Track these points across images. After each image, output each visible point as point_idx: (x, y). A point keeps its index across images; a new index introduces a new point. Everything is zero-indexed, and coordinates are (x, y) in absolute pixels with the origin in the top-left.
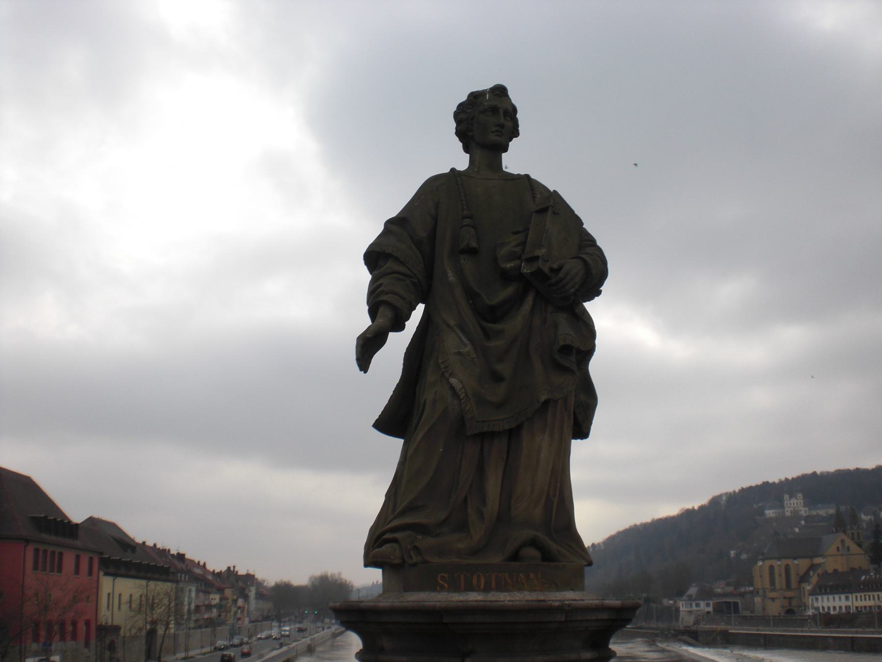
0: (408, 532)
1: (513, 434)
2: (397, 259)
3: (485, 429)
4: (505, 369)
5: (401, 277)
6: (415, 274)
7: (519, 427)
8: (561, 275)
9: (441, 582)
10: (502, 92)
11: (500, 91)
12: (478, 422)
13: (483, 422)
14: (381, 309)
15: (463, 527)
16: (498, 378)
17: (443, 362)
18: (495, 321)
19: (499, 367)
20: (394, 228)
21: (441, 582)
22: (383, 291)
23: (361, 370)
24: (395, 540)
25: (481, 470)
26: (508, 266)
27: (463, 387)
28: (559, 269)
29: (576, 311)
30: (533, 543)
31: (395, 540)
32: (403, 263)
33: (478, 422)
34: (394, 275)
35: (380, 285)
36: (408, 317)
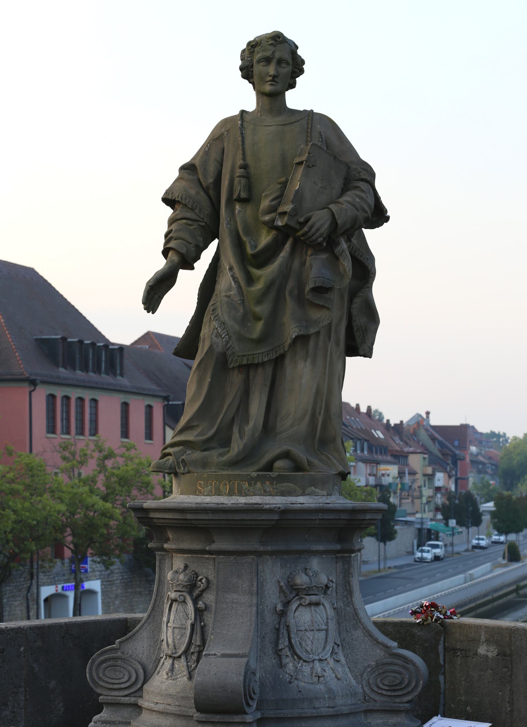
0: (181, 447)
3: (245, 362)
5: (190, 222)
6: (203, 219)
9: (199, 488)
10: (275, 40)
12: (239, 356)
13: (244, 356)
15: (226, 443)
21: (199, 488)
22: (172, 237)
26: (267, 218)
29: (335, 251)
30: (286, 455)
32: (192, 209)
33: (239, 356)
34: (184, 221)
36: (198, 258)
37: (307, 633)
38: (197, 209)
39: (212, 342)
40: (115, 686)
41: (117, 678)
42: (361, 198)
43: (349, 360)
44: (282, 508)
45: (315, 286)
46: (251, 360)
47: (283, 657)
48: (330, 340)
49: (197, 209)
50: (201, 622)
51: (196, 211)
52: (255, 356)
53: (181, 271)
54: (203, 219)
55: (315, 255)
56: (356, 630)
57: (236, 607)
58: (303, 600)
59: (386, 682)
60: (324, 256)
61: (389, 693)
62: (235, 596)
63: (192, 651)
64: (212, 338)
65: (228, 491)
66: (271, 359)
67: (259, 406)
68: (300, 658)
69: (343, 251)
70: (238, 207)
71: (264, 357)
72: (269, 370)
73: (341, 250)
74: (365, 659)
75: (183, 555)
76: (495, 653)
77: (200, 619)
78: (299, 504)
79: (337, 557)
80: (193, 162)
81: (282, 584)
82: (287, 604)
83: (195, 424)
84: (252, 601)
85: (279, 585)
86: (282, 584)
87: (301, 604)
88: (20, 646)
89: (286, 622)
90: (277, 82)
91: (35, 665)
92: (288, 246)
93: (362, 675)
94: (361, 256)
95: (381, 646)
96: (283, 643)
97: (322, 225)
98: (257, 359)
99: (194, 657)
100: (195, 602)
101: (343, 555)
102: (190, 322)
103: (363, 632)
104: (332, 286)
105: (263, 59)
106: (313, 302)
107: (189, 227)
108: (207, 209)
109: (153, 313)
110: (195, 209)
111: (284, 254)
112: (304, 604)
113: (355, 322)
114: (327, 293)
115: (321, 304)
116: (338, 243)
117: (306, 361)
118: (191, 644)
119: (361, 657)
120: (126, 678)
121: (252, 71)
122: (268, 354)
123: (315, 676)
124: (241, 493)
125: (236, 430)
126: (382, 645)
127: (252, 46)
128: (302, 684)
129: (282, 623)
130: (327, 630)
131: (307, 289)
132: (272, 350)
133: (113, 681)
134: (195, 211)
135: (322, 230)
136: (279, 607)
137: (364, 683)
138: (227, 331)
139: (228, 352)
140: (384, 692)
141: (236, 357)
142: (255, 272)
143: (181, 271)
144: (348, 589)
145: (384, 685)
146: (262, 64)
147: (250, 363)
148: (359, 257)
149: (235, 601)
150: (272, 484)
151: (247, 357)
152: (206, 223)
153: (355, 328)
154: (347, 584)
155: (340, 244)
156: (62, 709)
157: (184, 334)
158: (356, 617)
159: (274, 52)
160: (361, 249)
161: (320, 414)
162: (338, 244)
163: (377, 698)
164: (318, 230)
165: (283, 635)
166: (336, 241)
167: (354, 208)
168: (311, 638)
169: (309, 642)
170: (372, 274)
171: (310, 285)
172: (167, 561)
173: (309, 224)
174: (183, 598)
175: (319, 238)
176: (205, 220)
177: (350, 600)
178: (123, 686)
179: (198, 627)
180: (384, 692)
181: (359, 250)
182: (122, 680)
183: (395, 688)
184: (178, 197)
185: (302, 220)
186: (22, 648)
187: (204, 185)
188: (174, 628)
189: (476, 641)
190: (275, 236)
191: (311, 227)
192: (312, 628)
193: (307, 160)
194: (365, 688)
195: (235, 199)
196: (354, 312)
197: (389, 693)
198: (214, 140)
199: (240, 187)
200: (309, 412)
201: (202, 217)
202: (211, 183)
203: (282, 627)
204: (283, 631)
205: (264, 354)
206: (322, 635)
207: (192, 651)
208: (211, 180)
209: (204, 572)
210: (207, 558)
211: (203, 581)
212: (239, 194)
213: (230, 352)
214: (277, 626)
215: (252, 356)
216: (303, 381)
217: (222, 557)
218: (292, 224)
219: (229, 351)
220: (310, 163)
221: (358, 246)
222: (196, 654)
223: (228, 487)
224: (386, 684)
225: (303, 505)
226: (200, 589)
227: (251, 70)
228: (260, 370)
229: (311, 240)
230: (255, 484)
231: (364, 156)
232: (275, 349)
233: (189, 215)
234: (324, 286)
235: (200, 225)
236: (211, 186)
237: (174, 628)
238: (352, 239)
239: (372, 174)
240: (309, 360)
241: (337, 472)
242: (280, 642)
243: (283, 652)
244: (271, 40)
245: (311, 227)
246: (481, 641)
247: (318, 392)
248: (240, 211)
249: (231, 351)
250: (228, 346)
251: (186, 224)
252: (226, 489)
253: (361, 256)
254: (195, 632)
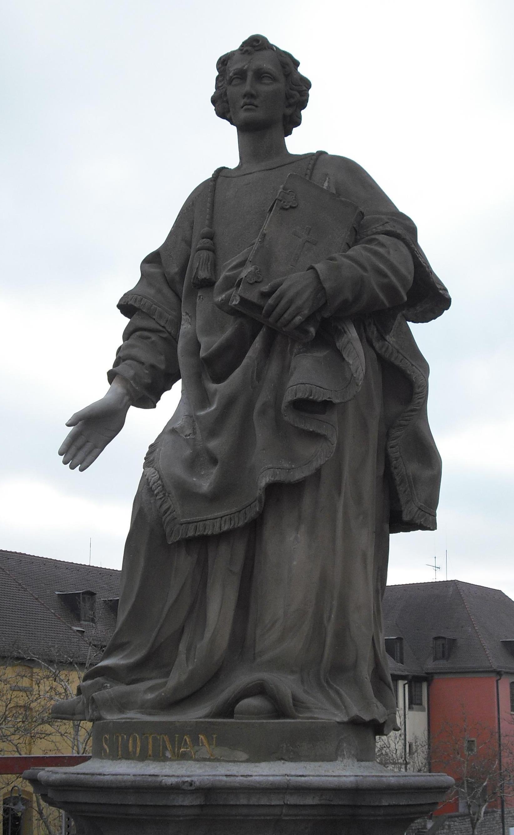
3: (191, 534)
5: (146, 334)
6: (163, 327)
10: (254, 47)
12: (182, 524)
13: (189, 523)
27: (160, 478)
29: (337, 344)
33: (182, 524)
34: (138, 333)
42: (376, 253)
44: (198, 783)
45: (295, 398)
46: (201, 529)
48: (340, 494)
52: (208, 522)
54: (163, 327)
60: (321, 354)
66: (236, 527)
67: (221, 608)
71: (223, 522)
78: (242, 776)
83: (125, 640)
90: (257, 106)
94: (401, 362)
97: (298, 294)
98: (211, 527)
104: (329, 398)
106: (296, 425)
109: (82, 470)
113: (396, 468)
114: (324, 414)
115: (311, 430)
116: (343, 331)
117: (297, 529)
122: (231, 520)
132: (240, 511)
134: (154, 317)
135: (299, 302)
139: (164, 518)
141: (178, 526)
142: (212, 386)
147: (199, 533)
148: (397, 363)
151: (195, 524)
152: (170, 333)
153: (398, 479)
155: (345, 332)
160: (400, 351)
162: (341, 333)
164: (291, 302)
166: (339, 327)
167: (356, 266)
170: (419, 387)
171: (289, 397)
173: (277, 293)
175: (295, 317)
181: (398, 352)
184: (131, 300)
185: (265, 288)
190: (236, 326)
191: (280, 298)
193: (280, 198)
196: (394, 453)
199: (198, 264)
202: (176, 273)
205: (223, 519)
212: (197, 273)
213: (168, 519)
215: (201, 523)
216: (295, 563)
219: (166, 515)
220: (285, 203)
221: (396, 347)
225: (250, 778)
228: (224, 549)
229: (282, 320)
231: (402, 207)
232: (244, 511)
234: (311, 398)
235: (161, 337)
238: (387, 337)
239: (412, 229)
240: (303, 528)
241: (346, 719)
245: (280, 298)
249: (169, 515)
253: (401, 362)
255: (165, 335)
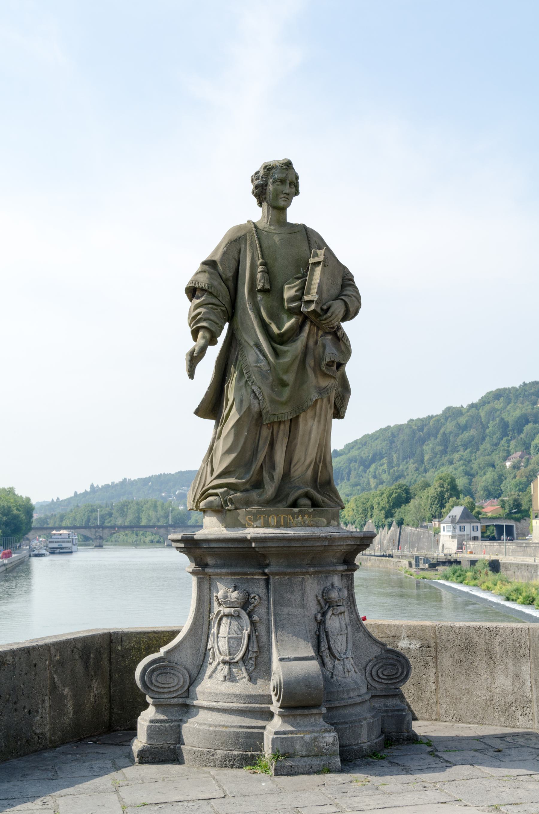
0: (225, 489)
1: (294, 422)
2: (211, 293)
4: (289, 378)
6: (224, 304)
7: (298, 417)
8: (329, 314)
10: (288, 166)
11: (288, 165)
14: (200, 334)
16: (283, 384)
17: (247, 373)
18: (282, 344)
19: (285, 377)
20: (206, 267)
23: (190, 378)
24: (216, 495)
25: (272, 445)
28: (328, 309)
29: (338, 334)
31: (216, 495)
32: (216, 297)
34: (210, 306)
35: (199, 314)
37: (338, 637)
38: (221, 297)
39: (250, 403)
40: (166, 690)
41: (168, 683)
43: (333, 420)
47: (325, 657)
49: (221, 297)
50: (255, 632)
51: (220, 298)
53: (209, 346)
54: (224, 304)
55: (324, 336)
56: (358, 633)
57: (292, 618)
58: (335, 611)
59: (386, 673)
61: (387, 682)
62: (290, 609)
63: (250, 656)
64: (250, 399)
65: (275, 524)
68: (335, 657)
69: (343, 334)
70: (259, 297)
72: (288, 426)
73: (342, 333)
74: (366, 656)
75: (230, 577)
76: (419, 645)
77: (255, 630)
79: (342, 575)
80: (213, 258)
81: (319, 598)
82: (324, 614)
83: (232, 469)
84: (304, 612)
85: (317, 599)
86: (319, 598)
87: (333, 614)
88: (46, 660)
89: (325, 628)
91: (55, 676)
92: (307, 328)
93: (365, 669)
95: (378, 645)
96: (324, 646)
99: (252, 662)
100: (250, 615)
101: (347, 573)
102: (209, 388)
103: (364, 634)
105: (278, 179)
107: (213, 310)
108: (226, 298)
110: (219, 297)
111: (304, 334)
112: (335, 613)
118: (247, 651)
119: (363, 654)
120: (176, 681)
121: (266, 190)
123: (347, 671)
124: (287, 525)
125: (265, 474)
126: (379, 644)
127: (268, 169)
128: (339, 678)
129: (321, 630)
130: (347, 634)
131: (324, 363)
133: (164, 686)
136: (319, 617)
137: (367, 675)
138: (263, 394)
140: (383, 681)
143: (209, 346)
144: (351, 600)
145: (383, 675)
146: (277, 183)
149: (290, 613)
150: (309, 516)
154: (350, 596)
156: (72, 712)
157: (204, 399)
158: (358, 622)
159: (287, 175)
161: (320, 462)
163: (377, 686)
165: (323, 639)
168: (341, 641)
169: (339, 644)
172: (205, 583)
173: (331, 310)
174: (237, 613)
176: (226, 306)
177: (353, 609)
178: (172, 689)
179: (254, 637)
180: (383, 681)
182: (172, 685)
183: (392, 677)
184: (205, 286)
185: (325, 307)
186: (47, 662)
187: (224, 276)
188: (229, 638)
189: (398, 637)
192: (341, 633)
194: (368, 678)
195: (260, 289)
197: (387, 682)
198: (231, 242)
200: (314, 461)
201: (224, 303)
203: (322, 633)
204: (323, 635)
206: (344, 638)
207: (250, 656)
208: (231, 274)
209: (255, 590)
210: (258, 579)
211: (257, 597)
214: (318, 633)
217: (277, 577)
218: (319, 310)
222: (254, 659)
223: (276, 520)
224: (386, 674)
226: (253, 605)
227: (265, 188)
230: (298, 517)
233: (214, 301)
235: (221, 309)
236: (231, 278)
237: (229, 638)
239: (352, 276)
240: (316, 419)
242: (322, 645)
243: (324, 654)
244: (285, 166)
246: (402, 637)
247: (320, 446)
248: (261, 300)
250: (264, 407)
251: (211, 308)
252: (274, 521)
254: (251, 641)
255: (224, 309)
